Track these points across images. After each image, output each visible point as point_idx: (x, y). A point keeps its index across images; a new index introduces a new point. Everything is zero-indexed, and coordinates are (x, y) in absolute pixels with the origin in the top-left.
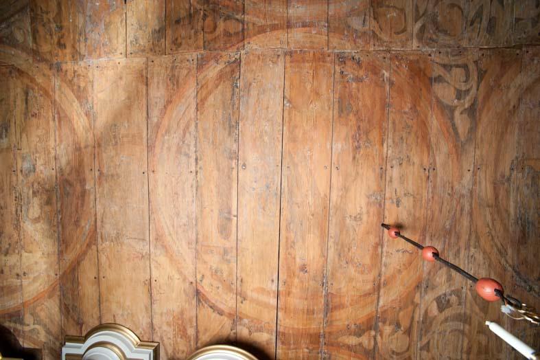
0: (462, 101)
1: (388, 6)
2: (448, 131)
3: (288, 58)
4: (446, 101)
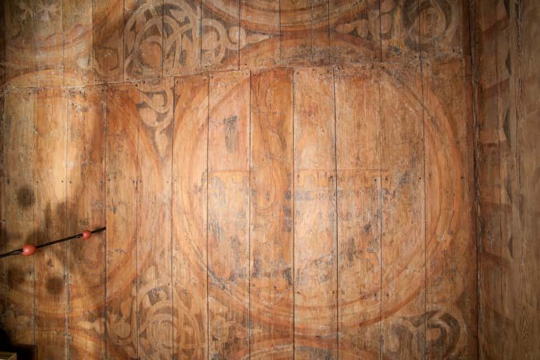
1: (105, 48)
2: (150, 148)
3: (36, 95)
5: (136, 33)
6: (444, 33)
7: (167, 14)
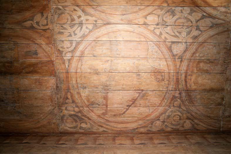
0: (35, 24)
2: (25, 19)
4: (35, 17)
5: (72, 11)
6: (67, 126)
7: (79, 25)
